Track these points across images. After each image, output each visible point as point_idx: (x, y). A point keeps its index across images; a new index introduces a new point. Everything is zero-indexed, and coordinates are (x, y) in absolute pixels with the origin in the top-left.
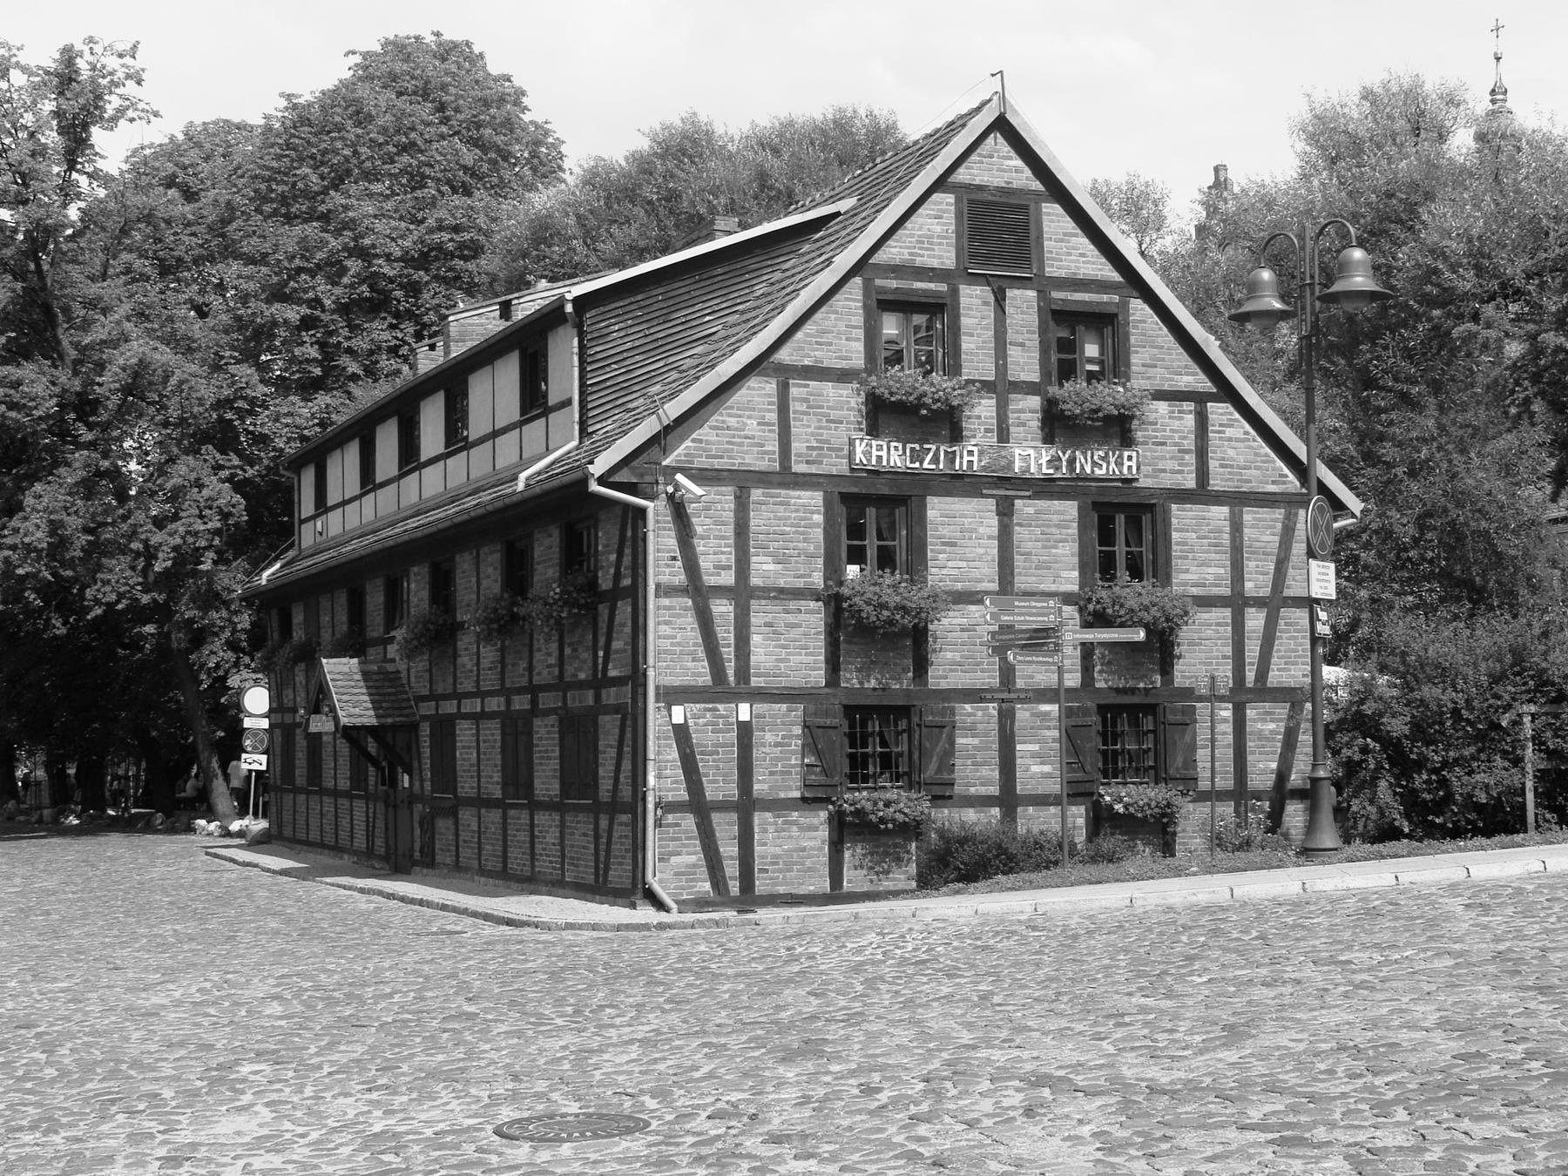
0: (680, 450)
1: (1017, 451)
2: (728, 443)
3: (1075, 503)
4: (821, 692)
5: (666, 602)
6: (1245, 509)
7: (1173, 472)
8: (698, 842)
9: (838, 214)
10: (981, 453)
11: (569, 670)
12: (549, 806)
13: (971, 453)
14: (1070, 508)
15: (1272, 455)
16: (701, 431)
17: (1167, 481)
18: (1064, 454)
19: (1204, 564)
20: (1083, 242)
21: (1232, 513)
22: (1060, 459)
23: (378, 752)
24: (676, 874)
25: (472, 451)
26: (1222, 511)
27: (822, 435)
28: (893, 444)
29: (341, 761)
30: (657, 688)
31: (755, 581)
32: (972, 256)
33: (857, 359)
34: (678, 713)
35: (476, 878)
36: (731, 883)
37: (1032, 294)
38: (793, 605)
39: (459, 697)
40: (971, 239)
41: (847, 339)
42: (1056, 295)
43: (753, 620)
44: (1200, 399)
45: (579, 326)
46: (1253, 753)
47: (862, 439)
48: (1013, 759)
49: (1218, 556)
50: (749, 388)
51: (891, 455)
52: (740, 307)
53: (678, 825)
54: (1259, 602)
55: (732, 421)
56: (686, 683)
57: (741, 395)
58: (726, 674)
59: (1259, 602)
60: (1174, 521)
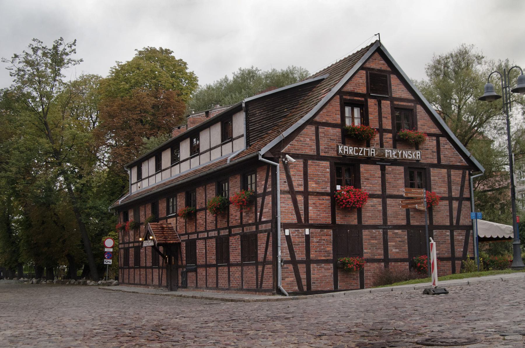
0: (286, 147)
2: (301, 146)
3: (403, 167)
4: (330, 225)
5: (283, 196)
6: (452, 170)
7: (430, 158)
8: (294, 274)
9: (324, 79)
10: (376, 151)
11: (245, 220)
12: (237, 265)
13: (373, 151)
14: (401, 169)
15: (458, 154)
16: (293, 142)
17: (429, 161)
19: (441, 187)
20: (402, 87)
21: (448, 171)
22: (398, 153)
23: (164, 252)
24: (287, 284)
25: (201, 156)
26: (444, 171)
27: (329, 144)
28: (350, 147)
29: (148, 257)
30: (281, 223)
31: (310, 190)
32: (371, 90)
33: (339, 120)
34: (287, 232)
35: (205, 290)
36: (304, 287)
37: (389, 102)
38: (321, 197)
39: (198, 233)
40: (371, 85)
41: (335, 114)
42: (396, 103)
43: (309, 202)
44: (437, 136)
45: (246, 112)
46: (456, 246)
47: (341, 146)
48: (387, 247)
49: (444, 185)
50: (307, 129)
51: (350, 150)
52: (295, 107)
53: (288, 268)
54: (456, 199)
55: (302, 139)
56: (290, 222)
57: (304, 131)
58: (301, 219)
59: (456, 199)
60: (431, 173)
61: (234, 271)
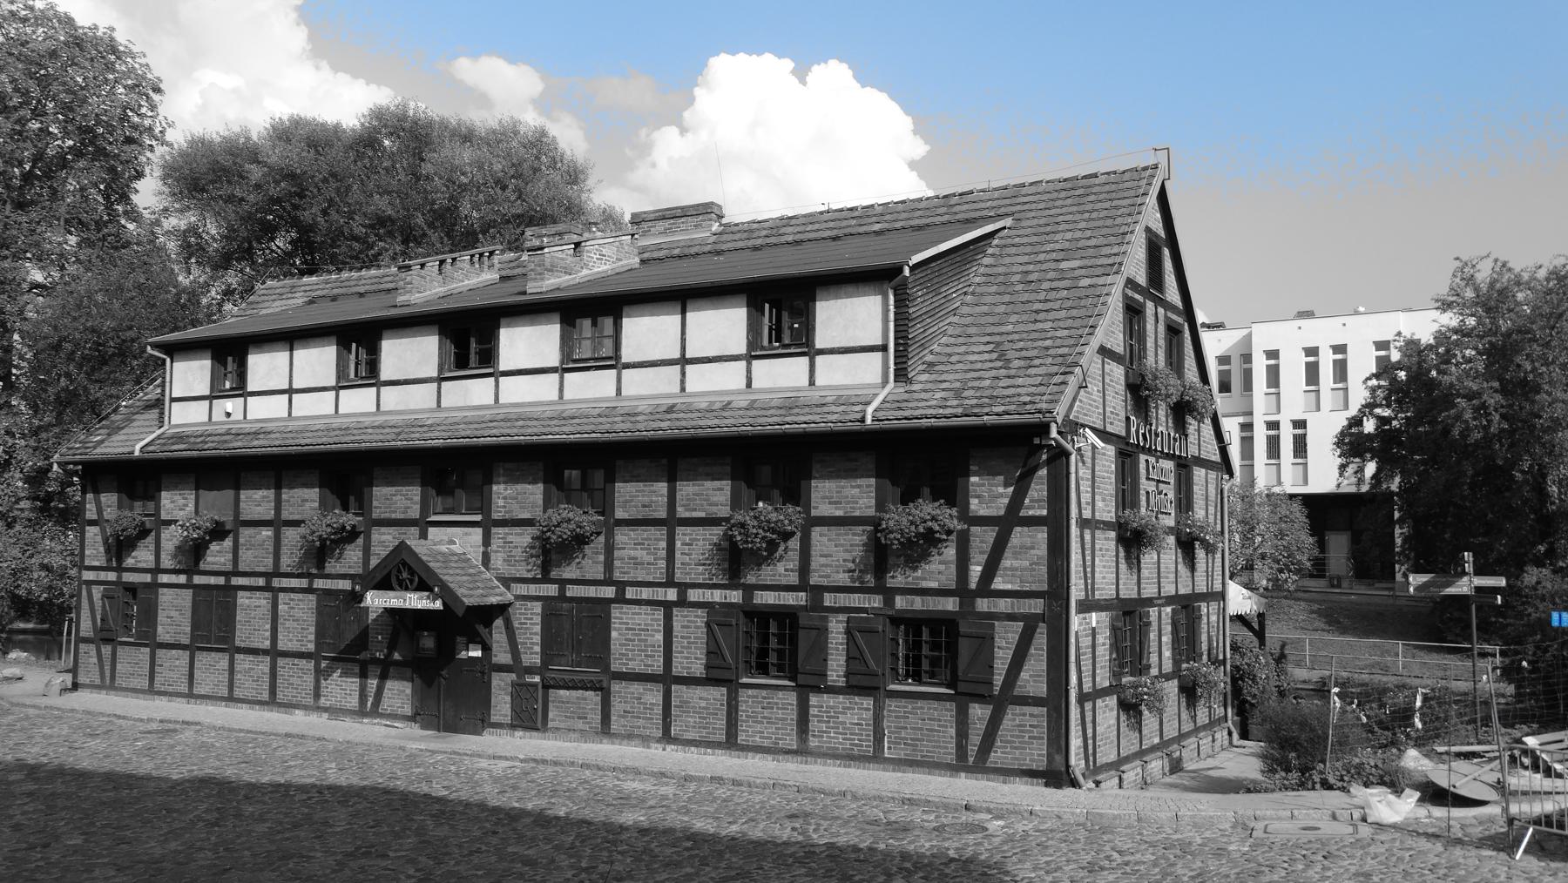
61: (832, 707)
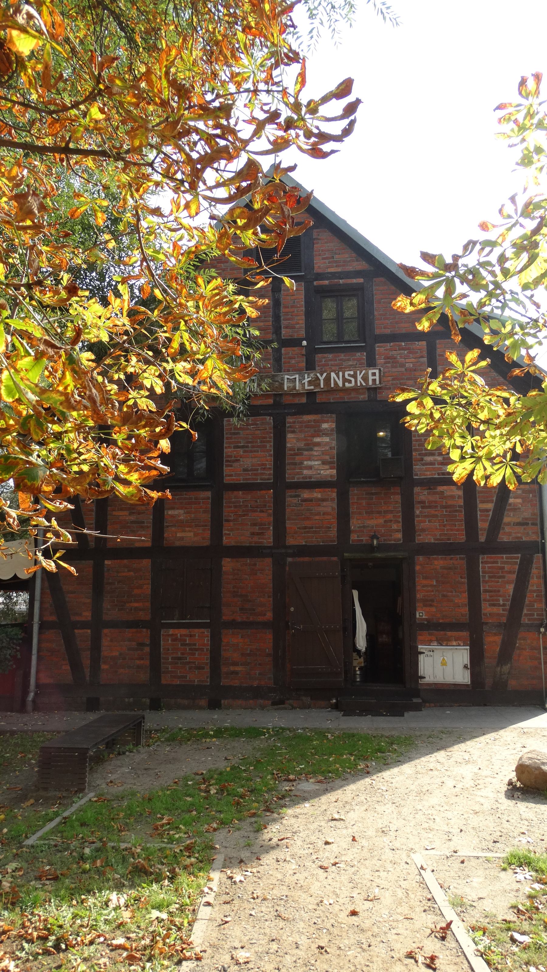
1: (286, 377)
18: (322, 375)
22: (318, 379)
